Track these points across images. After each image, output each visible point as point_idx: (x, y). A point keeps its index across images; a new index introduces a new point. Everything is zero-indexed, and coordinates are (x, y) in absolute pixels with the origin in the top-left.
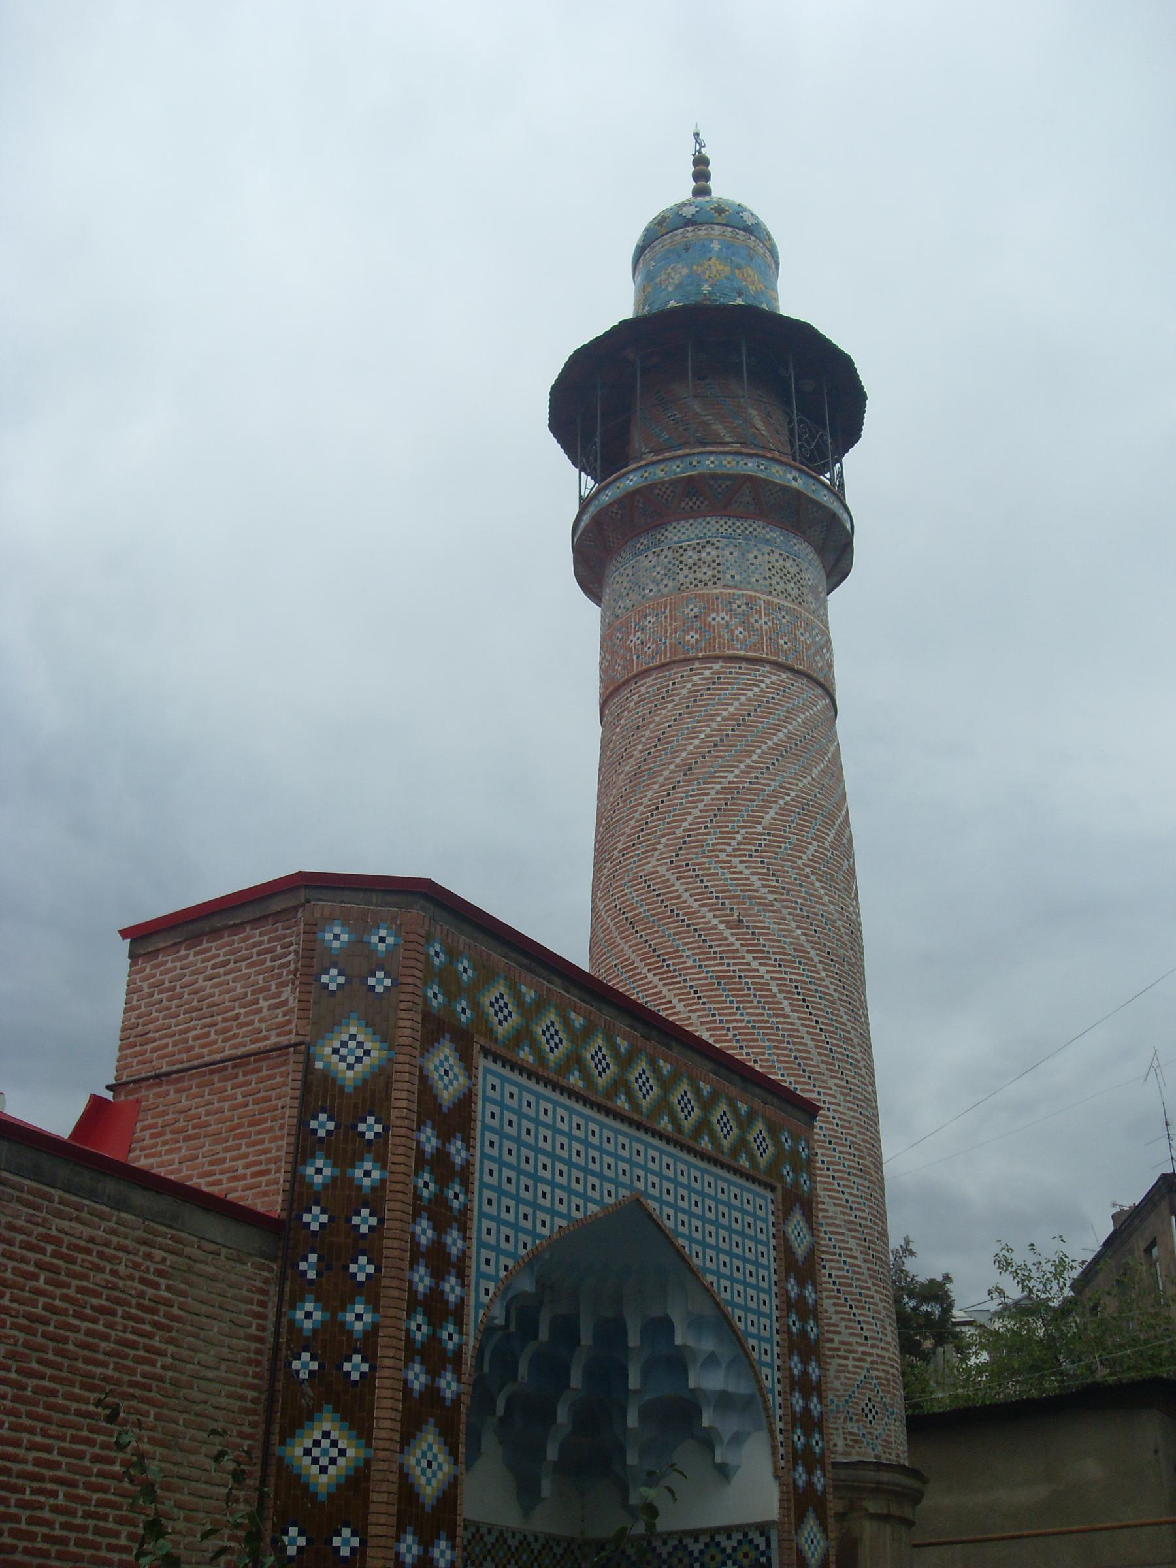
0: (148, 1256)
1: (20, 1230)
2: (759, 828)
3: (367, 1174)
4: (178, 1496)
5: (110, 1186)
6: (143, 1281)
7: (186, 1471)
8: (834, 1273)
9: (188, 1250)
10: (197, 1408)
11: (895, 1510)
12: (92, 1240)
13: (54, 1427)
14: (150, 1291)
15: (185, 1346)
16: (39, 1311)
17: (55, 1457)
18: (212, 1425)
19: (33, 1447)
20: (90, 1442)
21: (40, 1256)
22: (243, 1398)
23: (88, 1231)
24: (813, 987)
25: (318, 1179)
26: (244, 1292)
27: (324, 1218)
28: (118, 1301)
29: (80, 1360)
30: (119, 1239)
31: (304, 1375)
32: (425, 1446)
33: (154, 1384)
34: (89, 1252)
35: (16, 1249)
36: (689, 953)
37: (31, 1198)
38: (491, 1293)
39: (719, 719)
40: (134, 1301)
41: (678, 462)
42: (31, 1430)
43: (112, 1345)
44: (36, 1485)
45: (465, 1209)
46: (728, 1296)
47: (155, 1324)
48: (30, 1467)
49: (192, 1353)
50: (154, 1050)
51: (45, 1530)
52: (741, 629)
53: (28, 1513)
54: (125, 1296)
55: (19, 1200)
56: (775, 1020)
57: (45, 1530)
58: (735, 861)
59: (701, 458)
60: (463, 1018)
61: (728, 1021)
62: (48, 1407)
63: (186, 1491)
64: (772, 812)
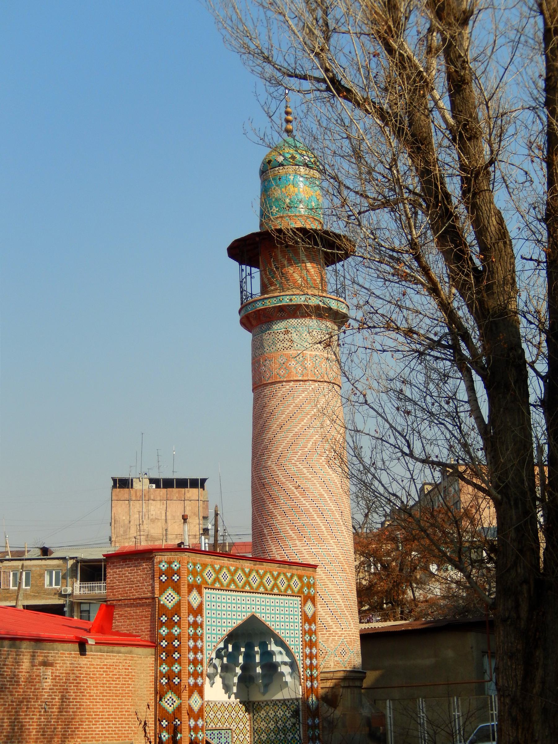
0: (126, 663)
2: (306, 449)
3: (176, 631)
5: (116, 648)
6: (125, 669)
8: (331, 608)
9: (135, 659)
11: (351, 684)
14: (127, 671)
16: (105, 682)
17: (111, 713)
19: (107, 712)
20: (118, 708)
23: (112, 661)
24: (325, 508)
25: (164, 633)
27: (166, 643)
31: (164, 683)
32: (194, 697)
34: (113, 665)
36: (282, 498)
39: (292, 406)
41: (275, 299)
42: (106, 708)
45: (202, 635)
46: (284, 635)
48: (107, 716)
50: (116, 592)
52: (300, 368)
55: (98, 658)
56: (311, 521)
58: (298, 463)
59: (283, 297)
60: (199, 582)
61: (296, 523)
62: (109, 702)
64: (311, 443)
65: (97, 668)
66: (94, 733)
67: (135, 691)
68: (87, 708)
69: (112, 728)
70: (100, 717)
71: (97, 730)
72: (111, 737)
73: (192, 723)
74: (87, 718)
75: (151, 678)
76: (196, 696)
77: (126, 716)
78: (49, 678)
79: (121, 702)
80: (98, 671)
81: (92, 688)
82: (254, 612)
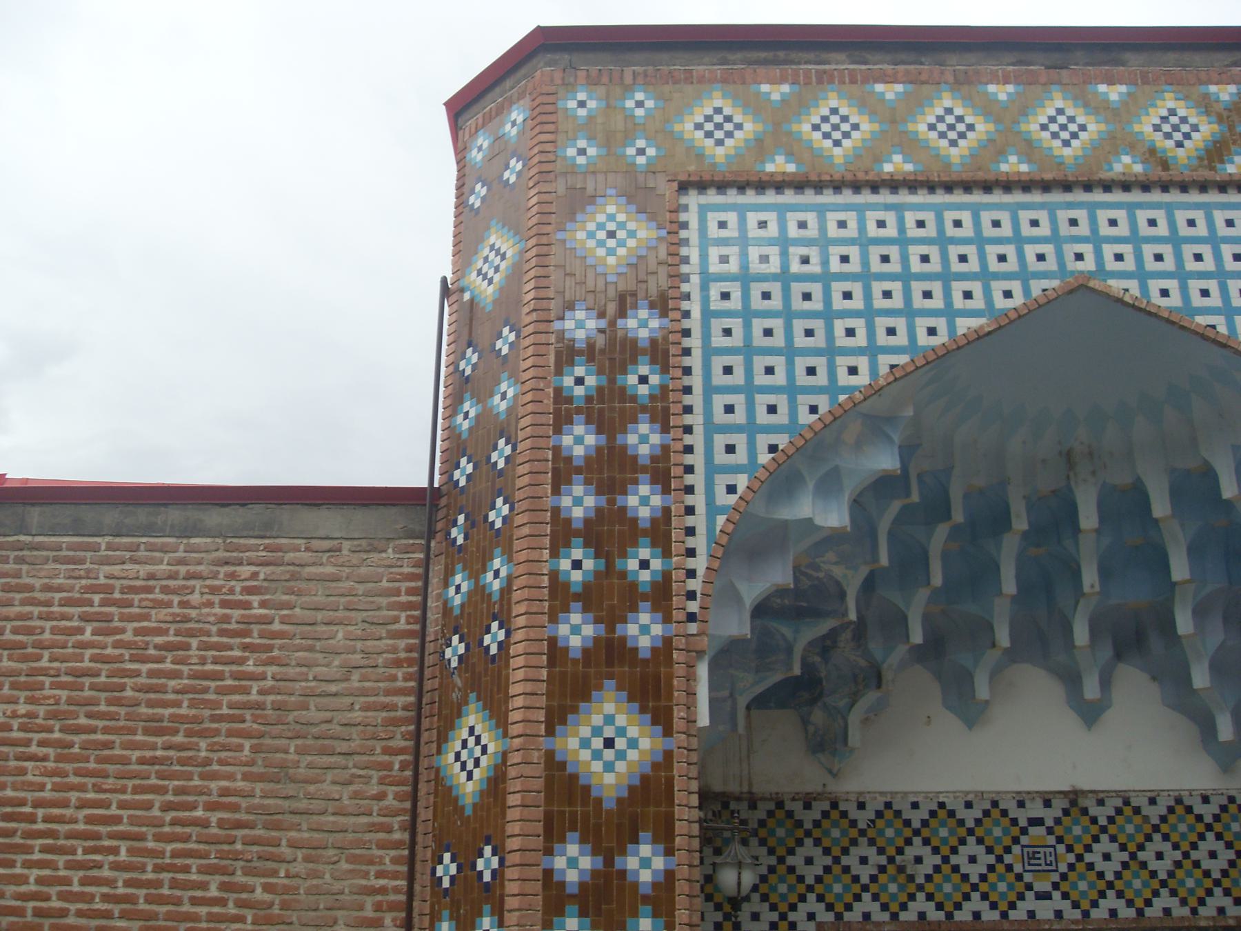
1: (59, 589)
4: (293, 834)
5: (174, 515)
7: (302, 805)
9: (290, 556)
10: (314, 730)
12: (151, 577)
13: (111, 780)
14: (236, 613)
15: (293, 663)
17: (114, 811)
18: (342, 747)
19: (83, 805)
22: (393, 707)
23: (144, 570)
26: (385, 584)
28: (191, 634)
29: (143, 705)
30: (189, 567)
32: (597, 720)
33: (248, 715)
34: (149, 590)
35: (55, 609)
37: (71, 553)
38: (741, 489)
40: (214, 629)
42: (81, 788)
43: (186, 681)
47: (245, 647)
48: (81, 826)
49: (304, 669)
51: (105, 890)
53: (81, 873)
54: (201, 625)
55: (56, 560)
57: (105, 890)
63: (304, 827)
65: (48, 603)
67: (277, 707)
70: (40, 826)
75: (402, 644)
77: (214, 830)
79: (182, 762)
80: (48, 617)
82: (1090, 275)
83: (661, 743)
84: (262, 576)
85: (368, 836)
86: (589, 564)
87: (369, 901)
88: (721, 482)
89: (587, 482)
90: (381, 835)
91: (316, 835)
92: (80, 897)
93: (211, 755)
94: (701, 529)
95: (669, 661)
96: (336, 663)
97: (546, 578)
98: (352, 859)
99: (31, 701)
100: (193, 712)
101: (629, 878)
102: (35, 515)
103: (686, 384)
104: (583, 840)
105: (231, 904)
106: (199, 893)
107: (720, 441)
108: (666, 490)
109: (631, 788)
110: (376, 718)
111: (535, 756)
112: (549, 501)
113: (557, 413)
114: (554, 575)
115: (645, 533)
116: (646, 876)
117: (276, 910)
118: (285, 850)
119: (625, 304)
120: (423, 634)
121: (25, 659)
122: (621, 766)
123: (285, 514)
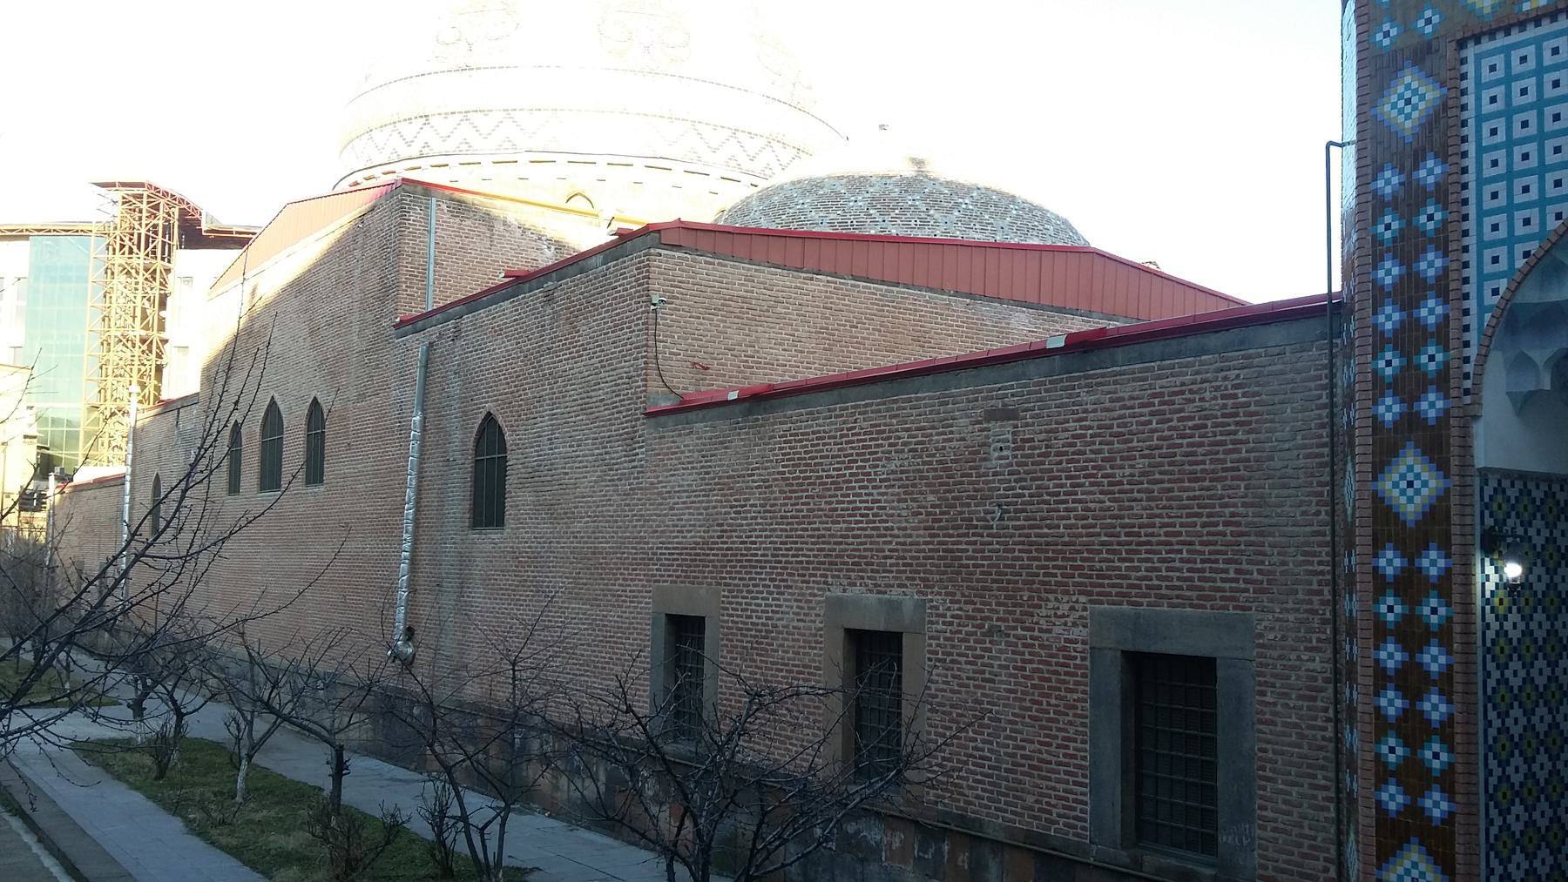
5: (1192, 342)
10: (1278, 473)
12: (1183, 384)
17: (1178, 529)
18: (1293, 483)
19: (1163, 525)
21: (1152, 408)
22: (1322, 455)
23: (1179, 380)
26: (1312, 373)
28: (1207, 418)
32: (1403, 469)
33: (1241, 466)
34: (1183, 393)
40: (1219, 413)
42: (1160, 516)
44: (1168, 548)
47: (1237, 424)
48: (1163, 538)
51: (1178, 574)
53: (1166, 565)
55: (1134, 380)
62: (1169, 499)
63: (1277, 534)
65: (1132, 407)
66: (1125, 582)
67: (1257, 460)
68: (1104, 518)
69: (1179, 570)
70: (1144, 539)
71: (1133, 574)
72: (1178, 597)
73: (1390, 562)
74: (1103, 544)
76: (1411, 462)
77: (1229, 538)
78: (1008, 448)
79: (1210, 497)
81: (1118, 462)
83: (1441, 483)
84: (1242, 377)
85: (1312, 539)
86: (1396, 362)
87: (1315, 579)
88: (1488, 287)
89: (1394, 303)
90: (1320, 538)
91: (1283, 539)
92: (1167, 579)
93: (1224, 492)
94: (1474, 326)
95: (1448, 427)
96: (1288, 429)
97: (1370, 375)
98: (1305, 554)
99: (1132, 467)
100: (1213, 467)
101: (1424, 573)
102: (1120, 353)
103: (1464, 212)
104: (1395, 549)
105: (1241, 582)
106: (1224, 576)
107: (1488, 254)
108: (1446, 302)
109: (1424, 514)
110: (1312, 463)
111: (1366, 495)
112: (1370, 321)
113: (1374, 254)
114: (1375, 372)
115: (1432, 334)
116: (1433, 571)
117: (1265, 585)
118: (1267, 549)
119: (1418, 159)
120: (1332, 405)
121: (1126, 441)
122: (1417, 499)
123: (1250, 332)
